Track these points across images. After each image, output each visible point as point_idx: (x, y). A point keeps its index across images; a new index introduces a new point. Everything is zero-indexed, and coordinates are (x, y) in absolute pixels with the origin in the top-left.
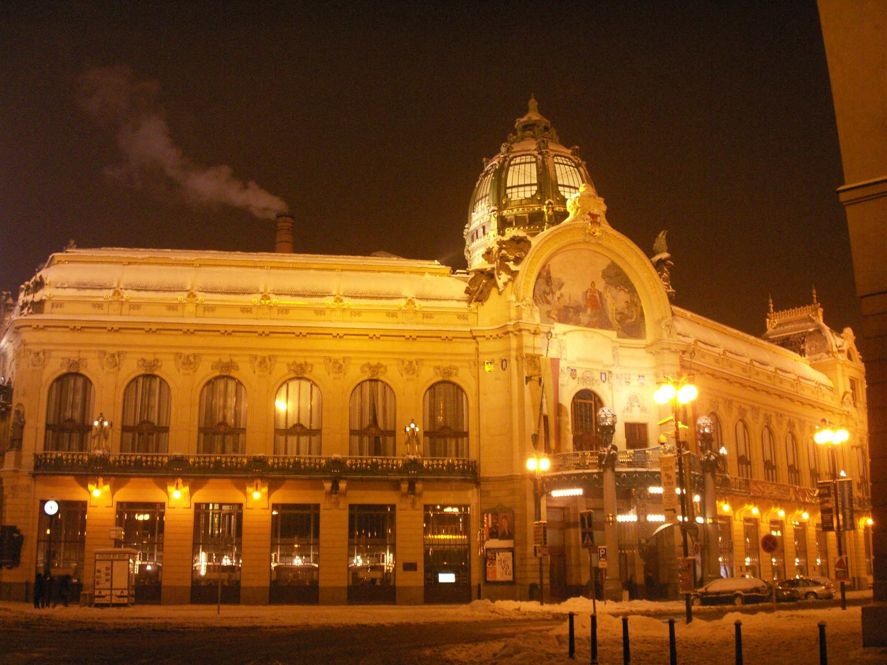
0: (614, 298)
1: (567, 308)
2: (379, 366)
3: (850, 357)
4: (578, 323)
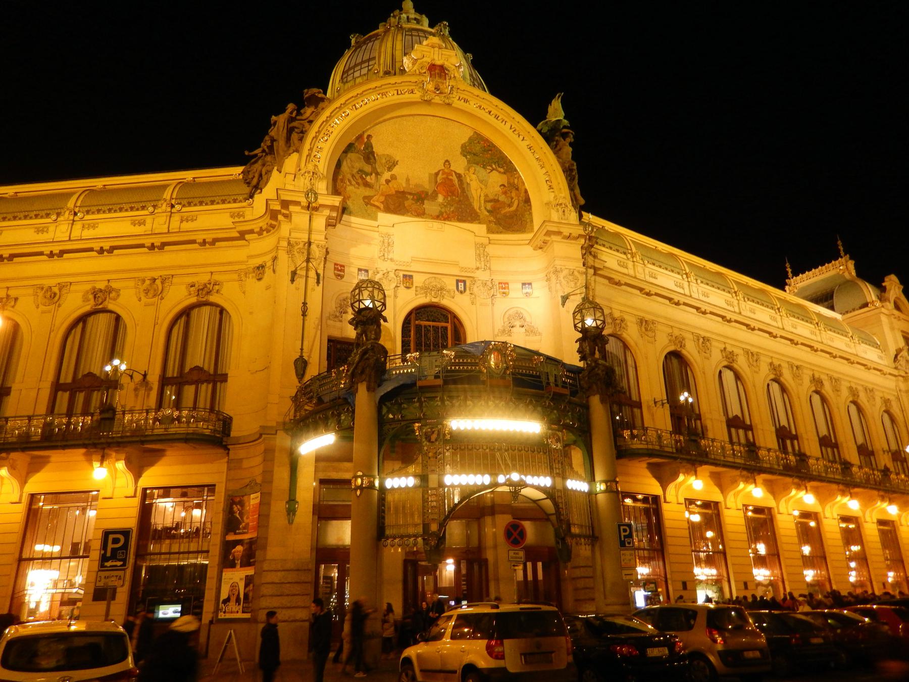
0: (481, 182)
1: (401, 195)
2: (109, 291)
3: (897, 307)
4: (421, 214)
